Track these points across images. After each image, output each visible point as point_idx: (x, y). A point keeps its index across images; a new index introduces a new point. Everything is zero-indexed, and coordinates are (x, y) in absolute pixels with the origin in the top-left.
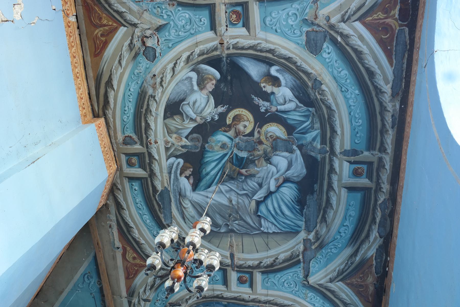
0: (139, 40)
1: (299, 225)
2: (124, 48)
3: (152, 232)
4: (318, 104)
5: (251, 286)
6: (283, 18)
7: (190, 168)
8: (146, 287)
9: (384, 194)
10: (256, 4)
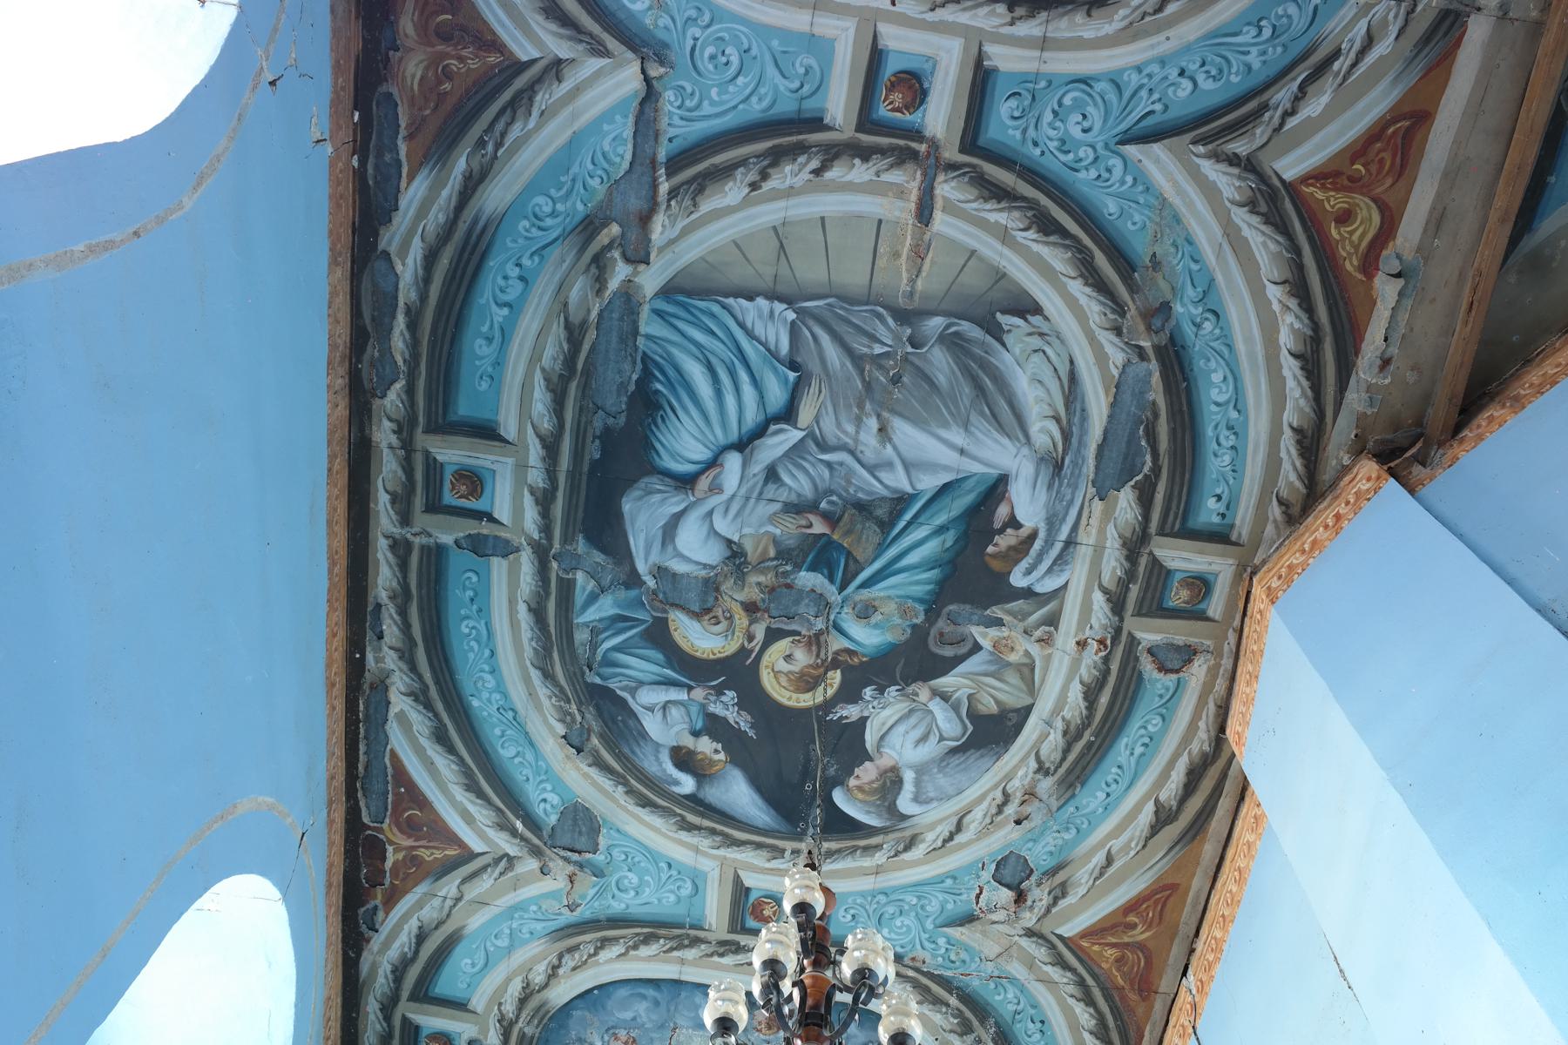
0: (1034, 902)
1: (659, 320)
2: (1082, 891)
3: (1217, 331)
5: (876, 56)
6: (649, 886)
7: (994, 556)
8: (1354, 65)
9: (388, 411)
10: (710, 924)
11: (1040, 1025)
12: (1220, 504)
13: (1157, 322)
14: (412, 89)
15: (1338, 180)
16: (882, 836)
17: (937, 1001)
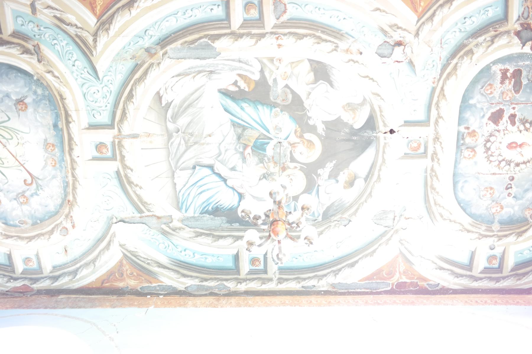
0: (401, 37)
1: (188, 211)
3: (152, 29)
4: (326, 224)
5: (94, 159)
7: (249, 87)
8: (57, 10)
11: (467, 19)
12: (214, 9)
13: (153, 51)
14: (138, 283)
15: (92, 2)
16: (374, 106)
17: (455, 68)
